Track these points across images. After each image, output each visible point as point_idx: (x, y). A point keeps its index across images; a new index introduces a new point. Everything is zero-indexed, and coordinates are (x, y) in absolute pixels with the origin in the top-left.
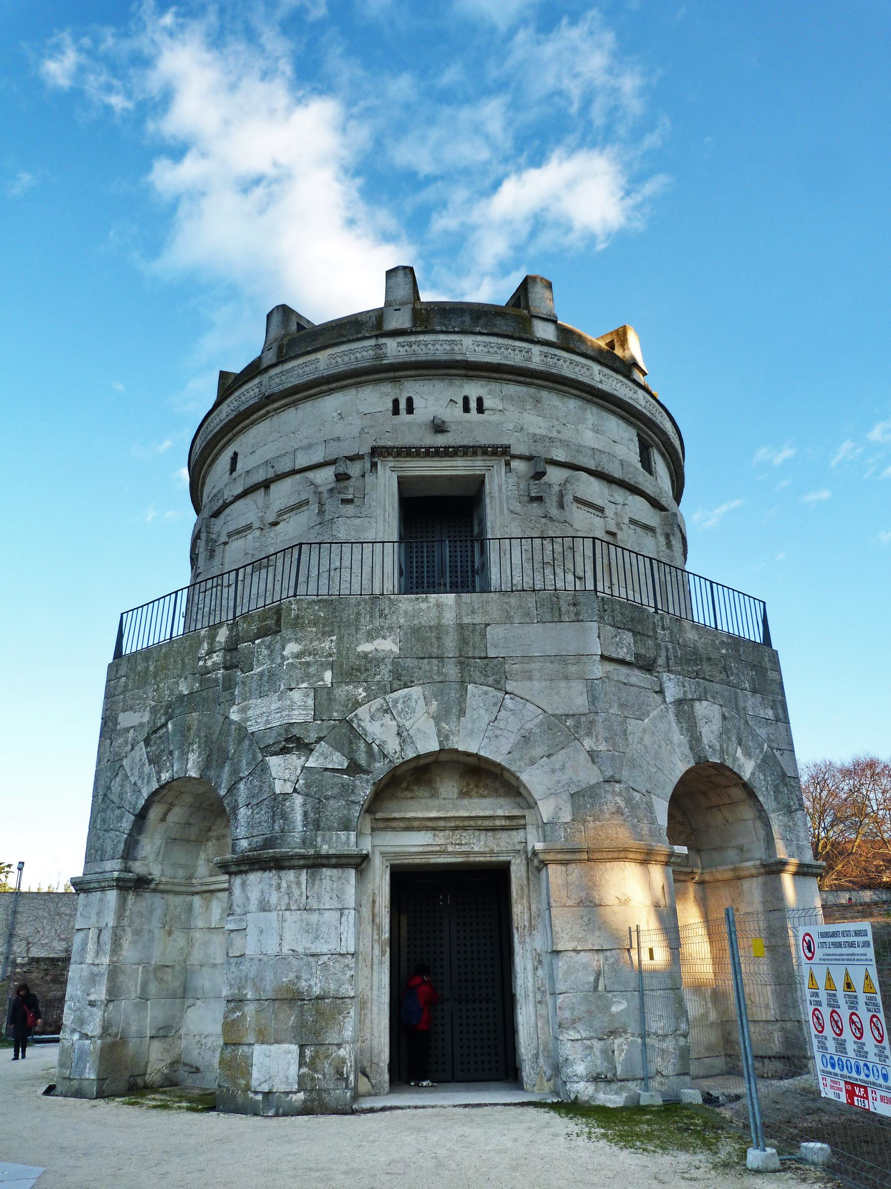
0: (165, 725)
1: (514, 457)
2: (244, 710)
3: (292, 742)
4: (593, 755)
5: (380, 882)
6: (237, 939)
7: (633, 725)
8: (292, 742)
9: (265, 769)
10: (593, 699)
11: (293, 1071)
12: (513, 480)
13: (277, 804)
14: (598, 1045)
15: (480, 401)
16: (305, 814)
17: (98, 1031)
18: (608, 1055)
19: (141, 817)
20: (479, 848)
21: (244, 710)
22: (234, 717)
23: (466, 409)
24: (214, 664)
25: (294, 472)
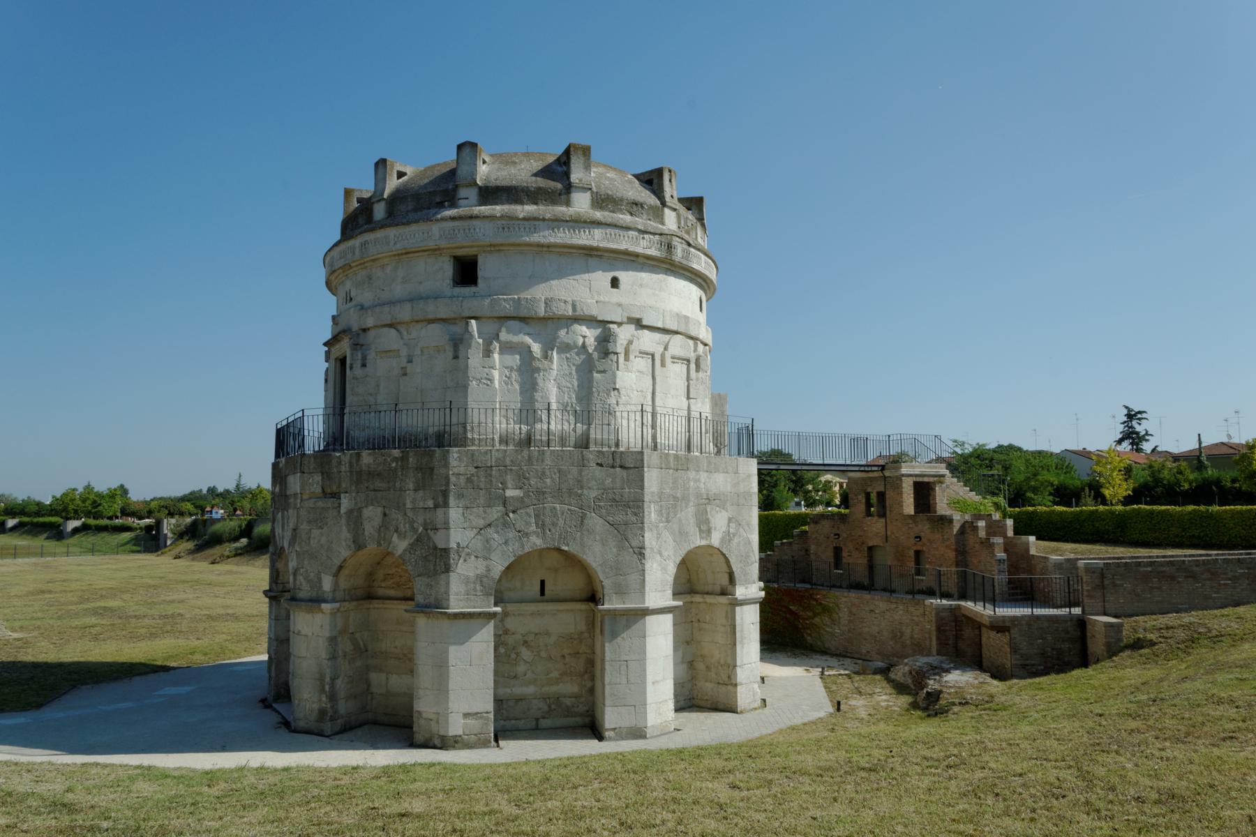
7: (316, 532)
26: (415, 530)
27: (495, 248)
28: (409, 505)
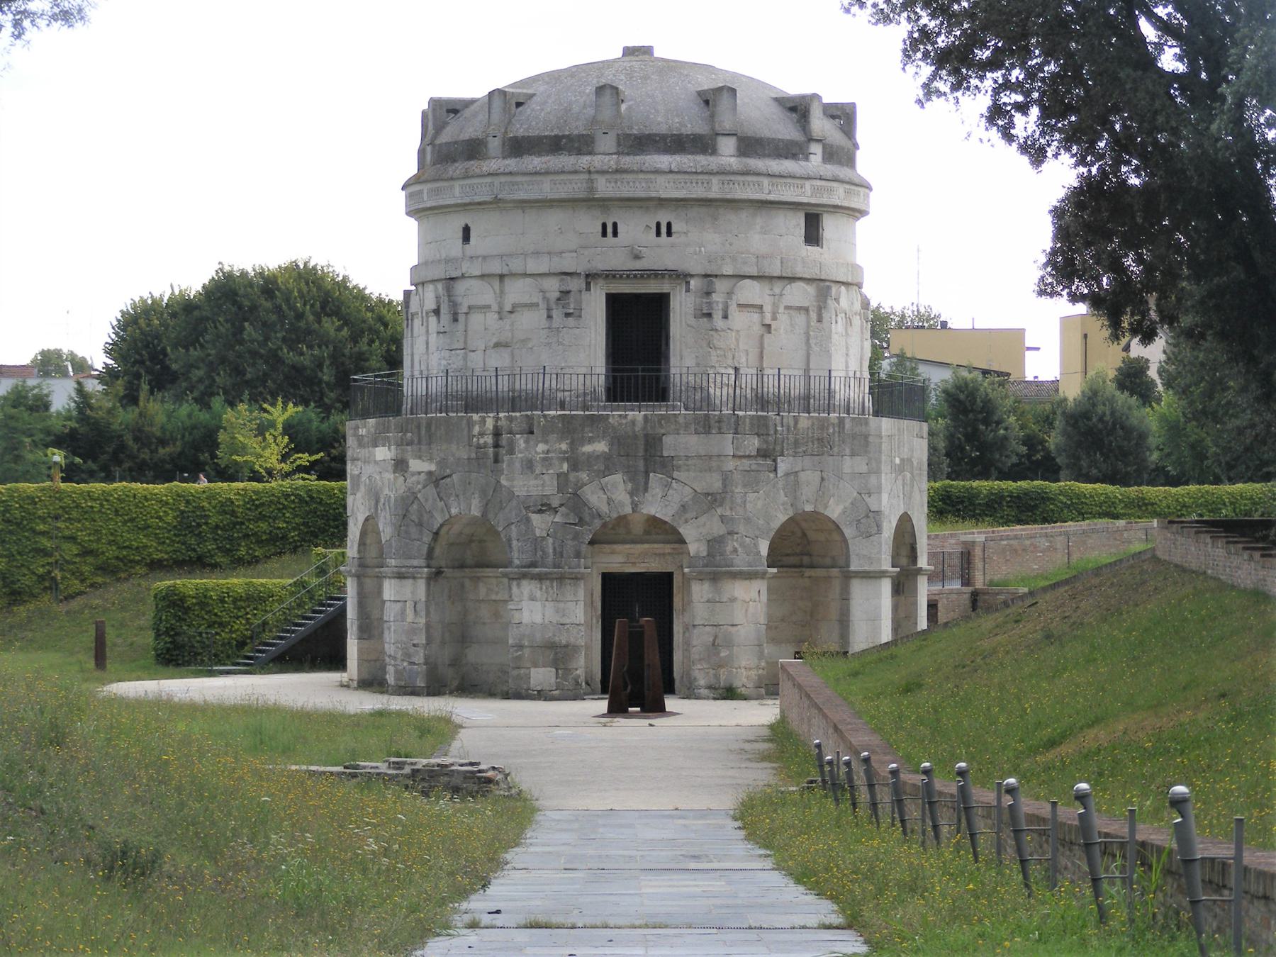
1: (692, 276)
6: (517, 614)
7: (751, 496)
9: (528, 520)
10: (725, 486)
11: (553, 680)
13: (537, 542)
14: (712, 672)
15: (669, 225)
16: (554, 549)
17: (422, 661)
18: (717, 677)
19: (437, 534)
21: (512, 480)
22: (504, 482)
23: (658, 234)
25: (525, 275)
27: (836, 209)
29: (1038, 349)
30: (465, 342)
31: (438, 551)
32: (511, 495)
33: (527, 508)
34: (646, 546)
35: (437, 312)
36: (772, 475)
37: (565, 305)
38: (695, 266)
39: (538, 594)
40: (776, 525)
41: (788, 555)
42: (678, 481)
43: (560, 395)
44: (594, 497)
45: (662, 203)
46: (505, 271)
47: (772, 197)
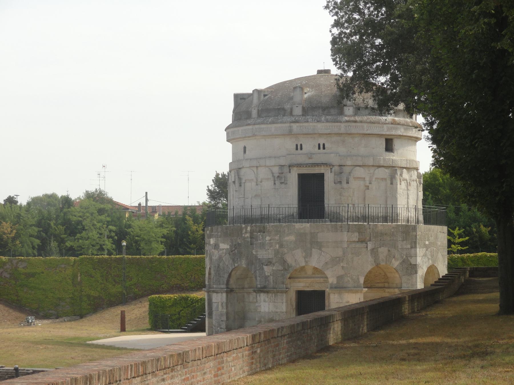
0: (234, 250)
1: (333, 166)
2: (257, 251)
3: (269, 263)
4: (343, 267)
5: (293, 295)
8: (269, 263)
9: (263, 269)
12: (333, 174)
13: (266, 277)
15: (324, 145)
17: (225, 327)
20: (317, 287)
21: (257, 251)
22: (254, 253)
23: (319, 148)
24: (247, 237)
26: (402, 257)
27: (400, 137)
28: (400, 247)
29: (146, 193)
30: (244, 195)
31: (232, 281)
32: (256, 257)
33: (262, 264)
34: (312, 279)
35: (234, 182)
36: (365, 249)
37: (280, 179)
38: (335, 160)
39: (267, 299)
40: (367, 270)
41: (379, 283)
42: (324, 252)
43: (278, 216)
44: (289, 260)
45: (321, 135)
46: (258, 165)
47: (369, 132)
